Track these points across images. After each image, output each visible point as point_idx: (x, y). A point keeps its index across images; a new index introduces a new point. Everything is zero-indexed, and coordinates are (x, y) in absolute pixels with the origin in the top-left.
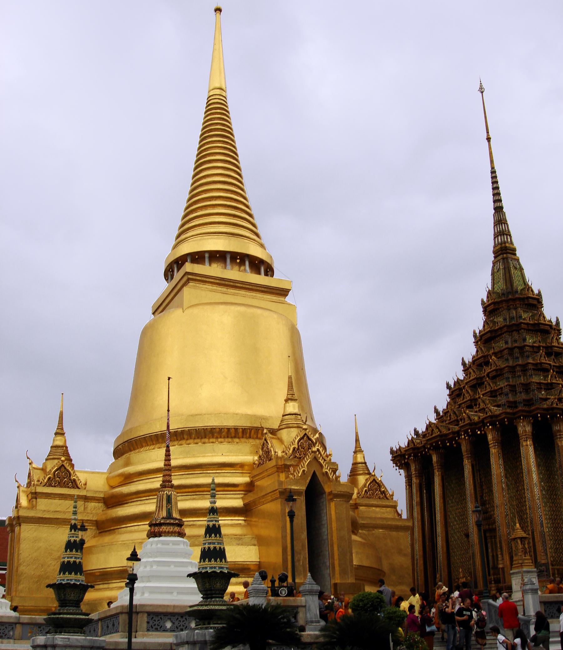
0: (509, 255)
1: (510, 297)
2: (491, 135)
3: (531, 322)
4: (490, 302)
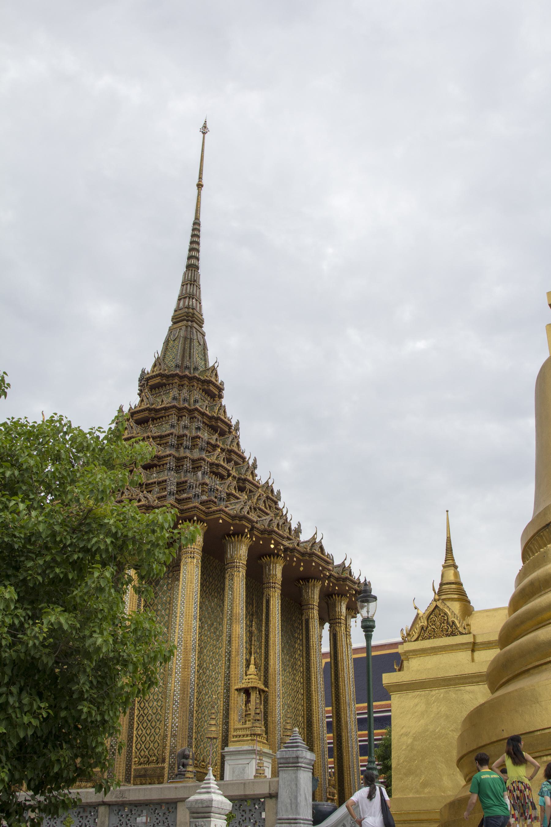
0: (195, 325)
1: (187, 373)
2: (204, 182)
3: (208, 413)
4: (155, 373)
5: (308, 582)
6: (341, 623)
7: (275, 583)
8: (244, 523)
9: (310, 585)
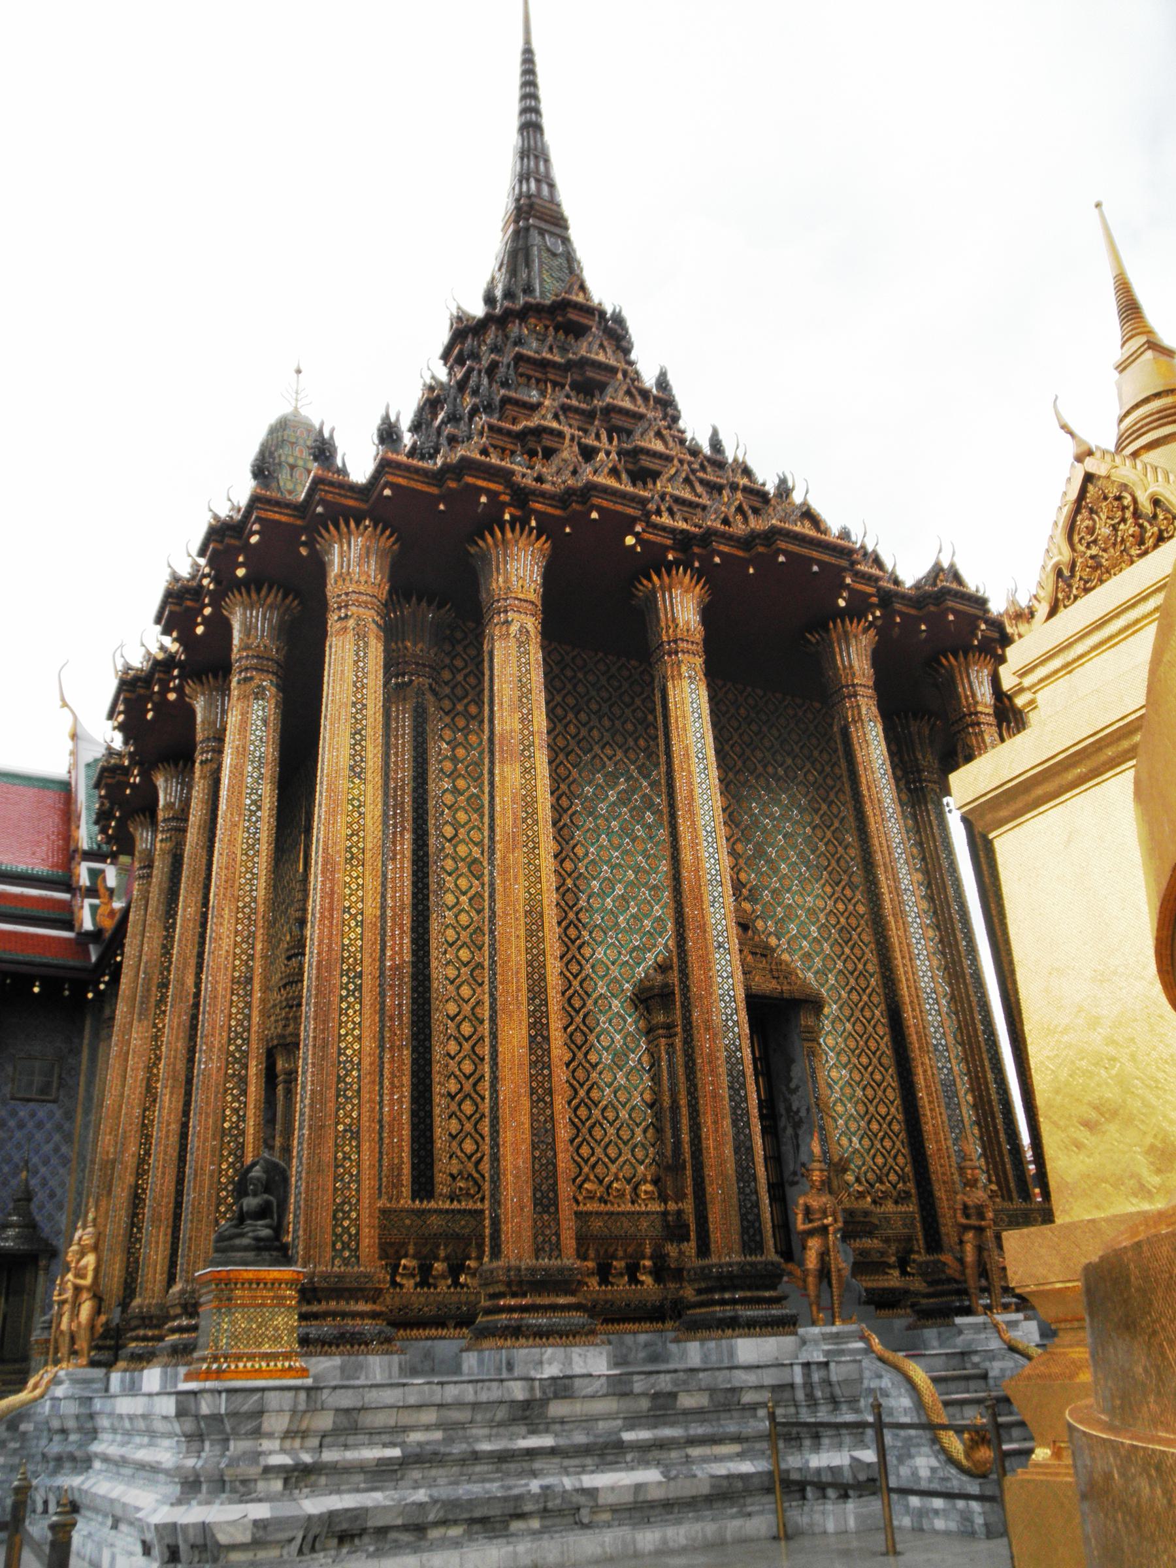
5: (827, 630)
6: (979, 724)
7: (675, 641)
8: (470, 480)
9: (834, 635)
